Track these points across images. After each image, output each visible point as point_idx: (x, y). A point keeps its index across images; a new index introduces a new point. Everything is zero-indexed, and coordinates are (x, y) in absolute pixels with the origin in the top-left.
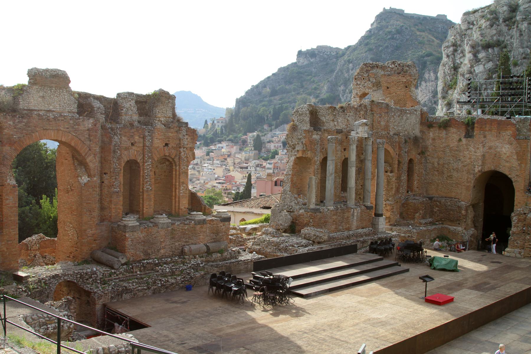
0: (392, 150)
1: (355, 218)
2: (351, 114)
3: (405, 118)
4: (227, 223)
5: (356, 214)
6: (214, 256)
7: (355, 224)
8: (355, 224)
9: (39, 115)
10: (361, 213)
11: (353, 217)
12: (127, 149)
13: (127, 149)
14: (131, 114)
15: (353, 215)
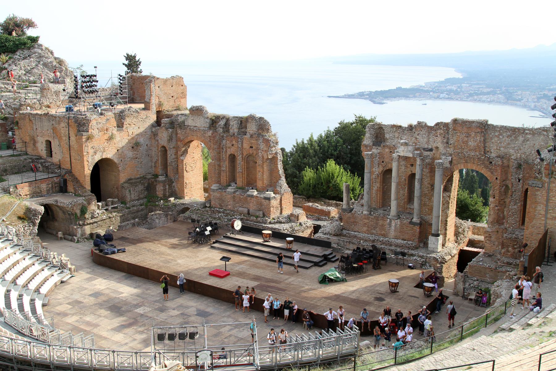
0: (489, 173)
1: (393, 228)
2: (422, 133)
3: (521, 139)
4: (267, 201)
5: (393, 224)
6: (252, 218)
7: (392, 233)
8: (392, 233)
9: (190, 128)
10: (402, 225)
11: (390, 226)
12: (229, 148)
13: (229, 148)
14: (234, 128)
15: (390, 224)
